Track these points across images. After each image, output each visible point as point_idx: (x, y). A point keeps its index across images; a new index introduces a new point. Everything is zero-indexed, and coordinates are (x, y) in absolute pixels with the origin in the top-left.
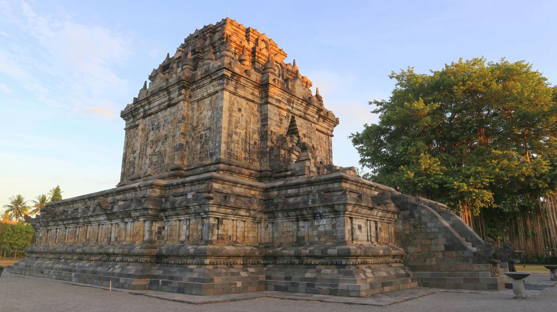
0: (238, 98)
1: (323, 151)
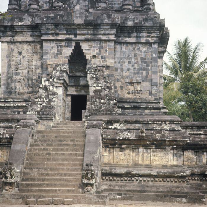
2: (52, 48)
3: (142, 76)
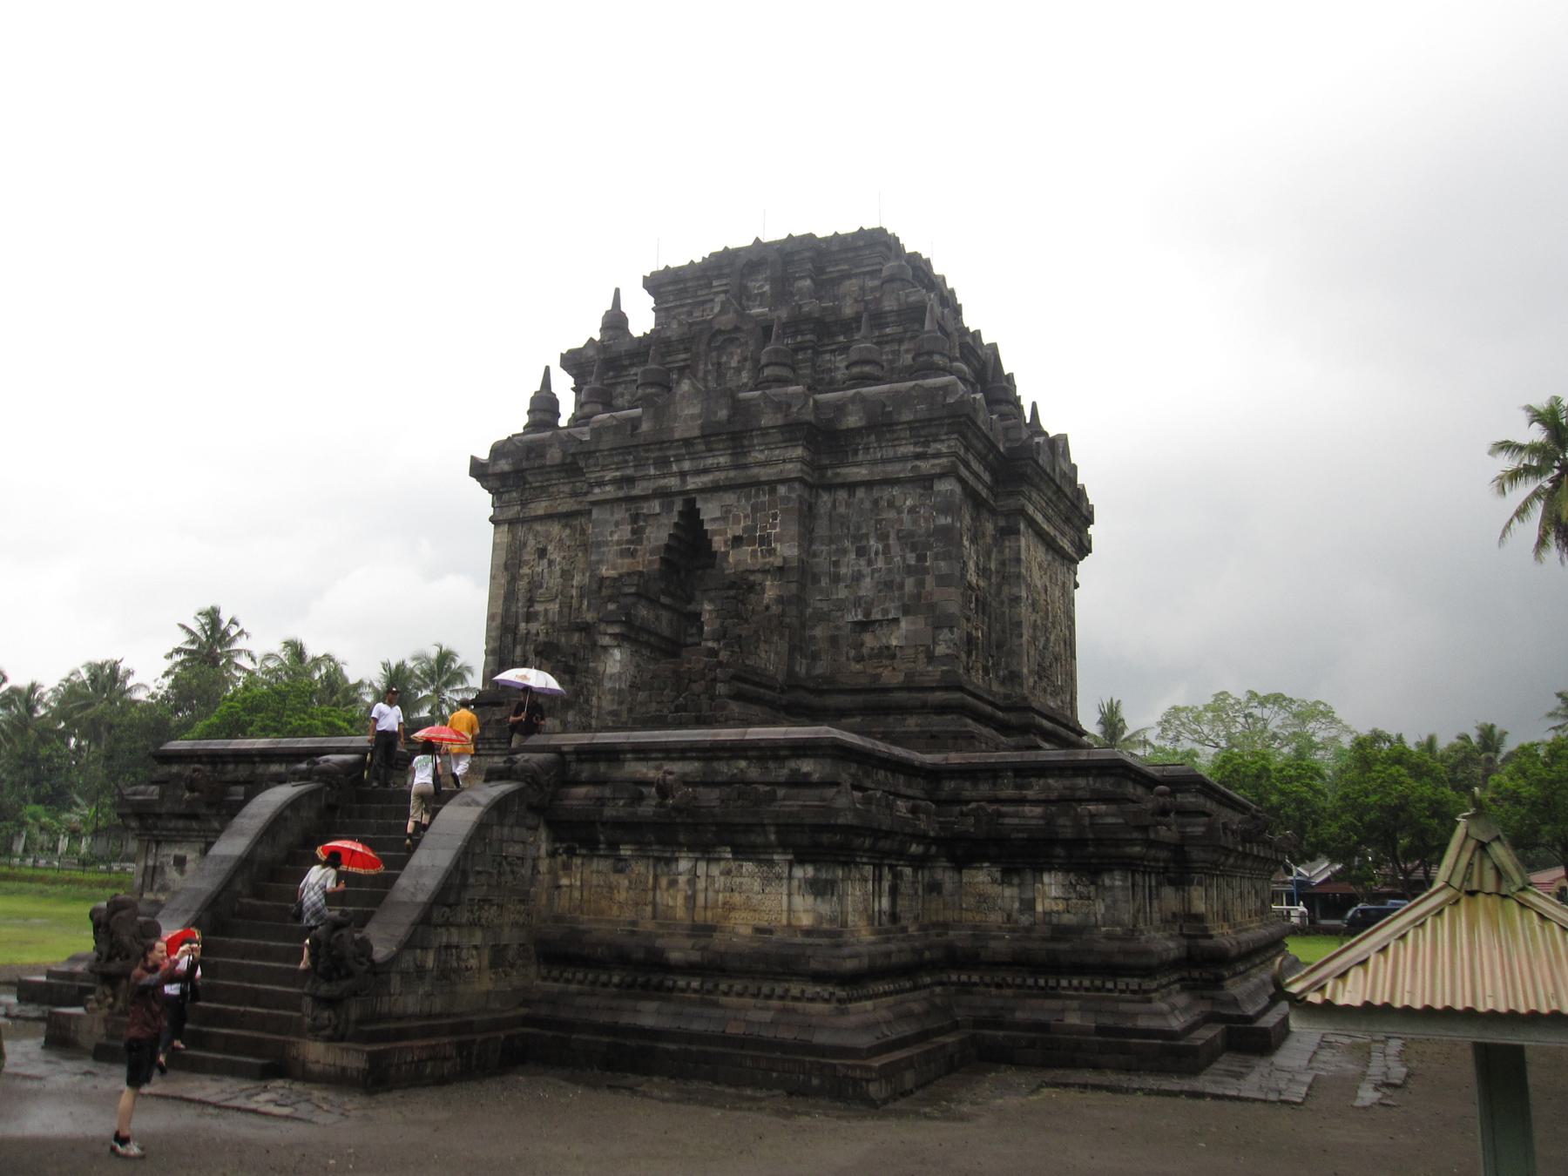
0: (538, 527)
1: (895, 548)
2: (617, 524)
3: (901, 598)
